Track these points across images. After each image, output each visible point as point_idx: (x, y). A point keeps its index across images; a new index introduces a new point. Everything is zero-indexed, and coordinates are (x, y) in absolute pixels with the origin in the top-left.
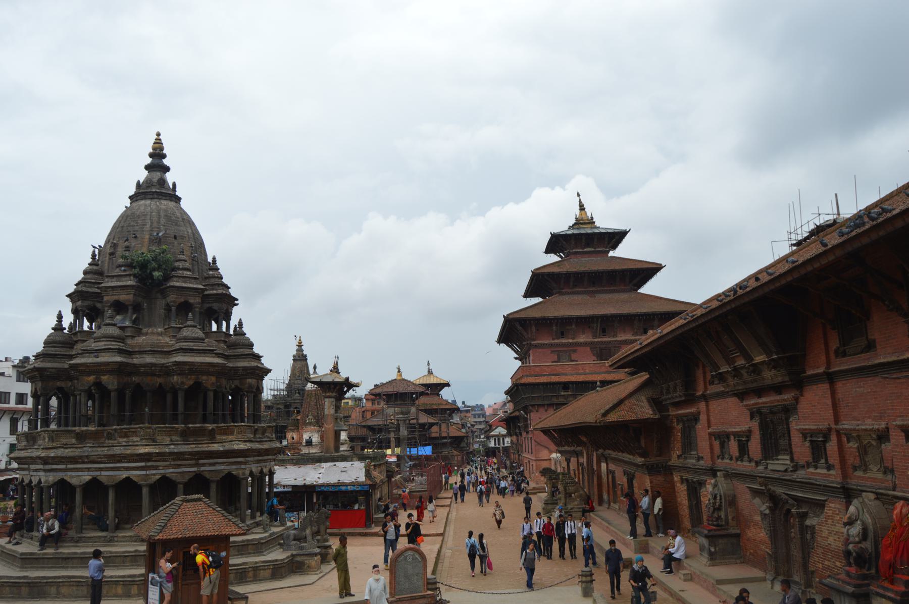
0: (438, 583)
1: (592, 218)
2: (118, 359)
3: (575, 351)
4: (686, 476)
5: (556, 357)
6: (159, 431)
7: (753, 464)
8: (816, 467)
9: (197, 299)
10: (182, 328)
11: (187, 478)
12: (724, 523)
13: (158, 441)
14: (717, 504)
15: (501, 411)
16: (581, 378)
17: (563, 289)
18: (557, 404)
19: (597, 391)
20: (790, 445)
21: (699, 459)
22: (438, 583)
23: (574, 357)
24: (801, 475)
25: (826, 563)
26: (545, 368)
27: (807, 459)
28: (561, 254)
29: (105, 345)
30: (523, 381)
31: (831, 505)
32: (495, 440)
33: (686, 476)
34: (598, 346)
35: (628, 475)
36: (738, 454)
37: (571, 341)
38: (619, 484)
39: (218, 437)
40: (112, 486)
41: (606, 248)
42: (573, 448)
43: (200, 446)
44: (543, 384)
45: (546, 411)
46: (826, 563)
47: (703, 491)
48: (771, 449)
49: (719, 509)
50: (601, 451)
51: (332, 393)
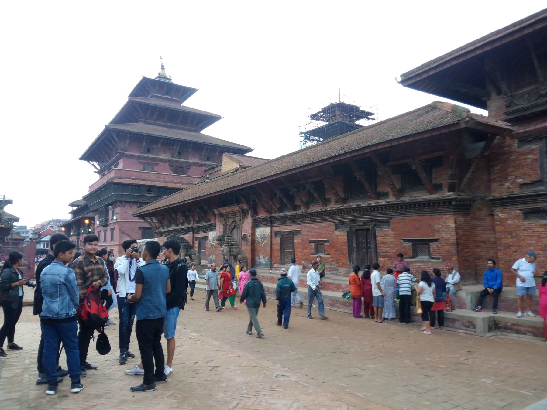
1: (170, 77)
3: (157, 165)
5: (142, 167)
16: (163, 185)
17: (147, 119)
18: (141, 203)
19: (207, 182)
23: (156, 168)
26: (135, 173)
30: (117, 180)
32: (44, 244)
35: (351, 228)
37: (155, 157)
41: (180, 99)
42: (186, 226)
45: (131, 207)
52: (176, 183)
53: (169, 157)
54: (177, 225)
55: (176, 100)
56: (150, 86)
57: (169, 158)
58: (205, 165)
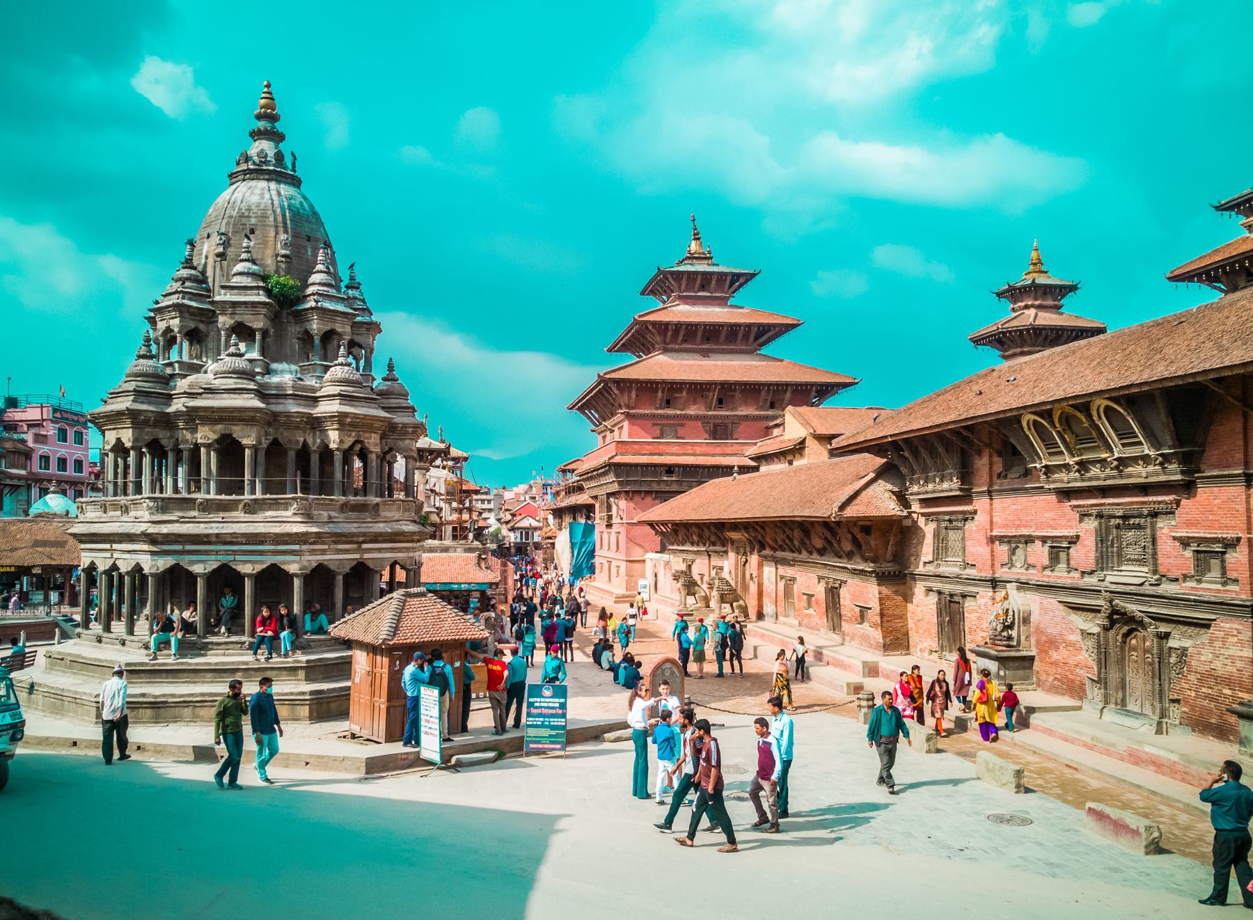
0: (693, 703)
1: (709, 252)
2: (257, 403)
3: (683, 425)
4: (937, 585)
5: (659, 432)
6: (316, 504)
7: (1076, 575)
8: (1199, 581)
9: (346, 326)
10: (332, 366)
11: (347, 570)
12: (1015, 643)
13: (315, 517)
14: (1009, 620)
15: (527, 497)
17: (668, 344)
18: (657, 492)
20: (1154, 554)
21: (966, 565)
22: (693, 703)
23: (681, 431)
24: (1167, 588)
25: (1204, 690)
27: (1184, 572)
28: (665, 297)
29: (235, 383)
30: (618, 459)
31: (1222, 625)
32: (522, 532)
33: (937, 585)
34: (712, 421)
36: (1047, 562)
37: (678, 412)
38: (804, 594)
39: (383, 514)
40: (249, 576)
43: (363, 525)
44: (642, 465)
45: (643, 499)
46: (1204, 690)
47: (969, 604)
48: (1107, 556)
49: (1011, 627)
50: (767, 552)
51: (425, 462)
52: (714, 455)
53: (703, 408)
54: (692, 544)
55: (720, 297)
56: (673, 282)
57: (702, 412)
58: (767, 418)
